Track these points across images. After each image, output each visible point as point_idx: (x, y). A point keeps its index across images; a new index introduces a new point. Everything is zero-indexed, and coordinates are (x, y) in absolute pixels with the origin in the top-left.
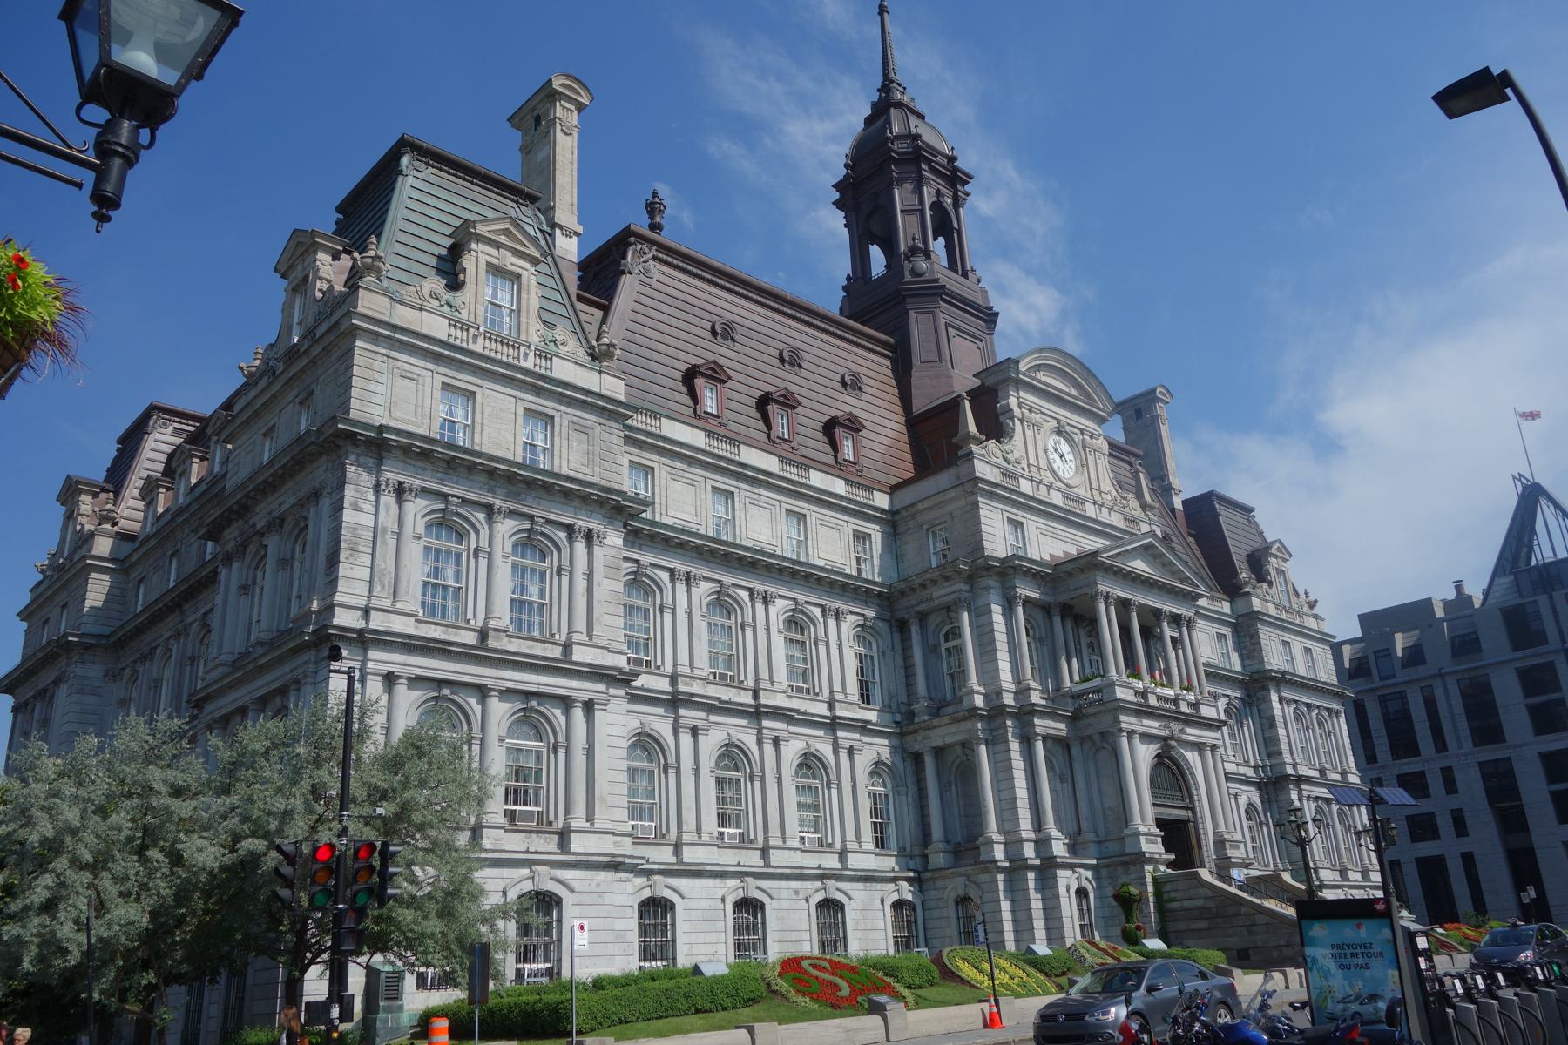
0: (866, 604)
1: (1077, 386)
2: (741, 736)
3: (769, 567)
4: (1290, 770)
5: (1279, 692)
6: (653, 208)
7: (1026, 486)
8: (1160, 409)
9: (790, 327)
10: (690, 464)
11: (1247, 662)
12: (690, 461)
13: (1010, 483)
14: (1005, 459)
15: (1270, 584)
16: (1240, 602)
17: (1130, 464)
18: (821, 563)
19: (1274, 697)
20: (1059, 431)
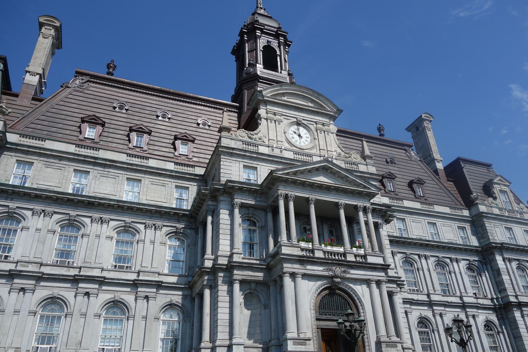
0: (179, 221)
1: (312, 101)
2: (61, 293)
3: (100, 204)
4: (512, 299)
5: (502, 255)
6: (111, 67)
7: (262, 150)
8: (426, 124)
9: (192, 108)
10: (60, 160)
11: (482, 241)
12: (61, 158)
13: (251, 148)
14: (250, 138)
15: (495, 198)
16: (474, 209)
17: (405, 150)
18: (146, 202)
19: (499, 259)
20: (298, 124)
